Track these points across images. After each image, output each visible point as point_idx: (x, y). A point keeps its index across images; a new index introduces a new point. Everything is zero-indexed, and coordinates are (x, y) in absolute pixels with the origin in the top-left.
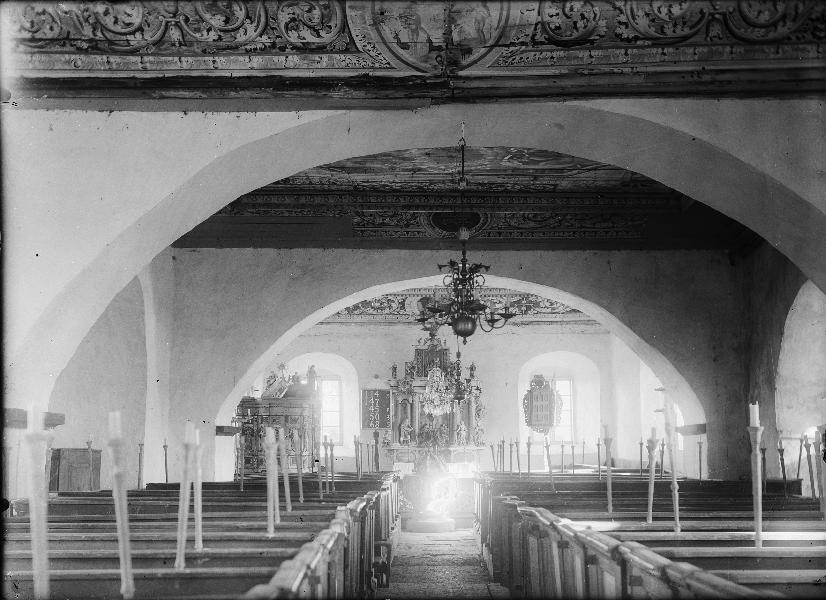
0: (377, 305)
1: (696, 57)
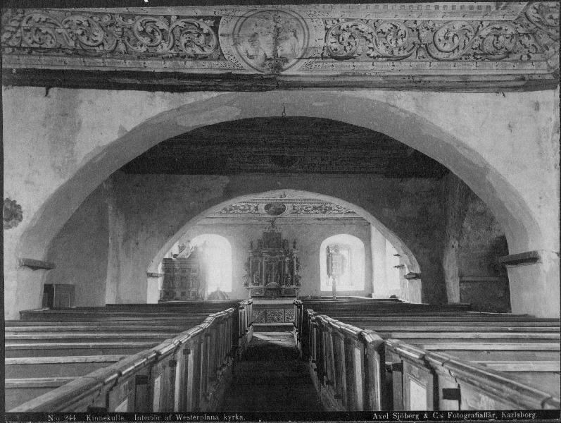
0: (242, 208)
1: (411, 68)
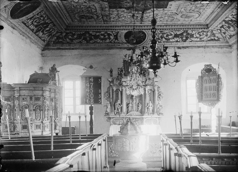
0: (102, 37)
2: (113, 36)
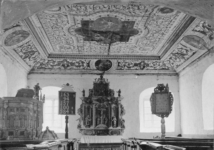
0: (77, 64)
2: (86, 63)
